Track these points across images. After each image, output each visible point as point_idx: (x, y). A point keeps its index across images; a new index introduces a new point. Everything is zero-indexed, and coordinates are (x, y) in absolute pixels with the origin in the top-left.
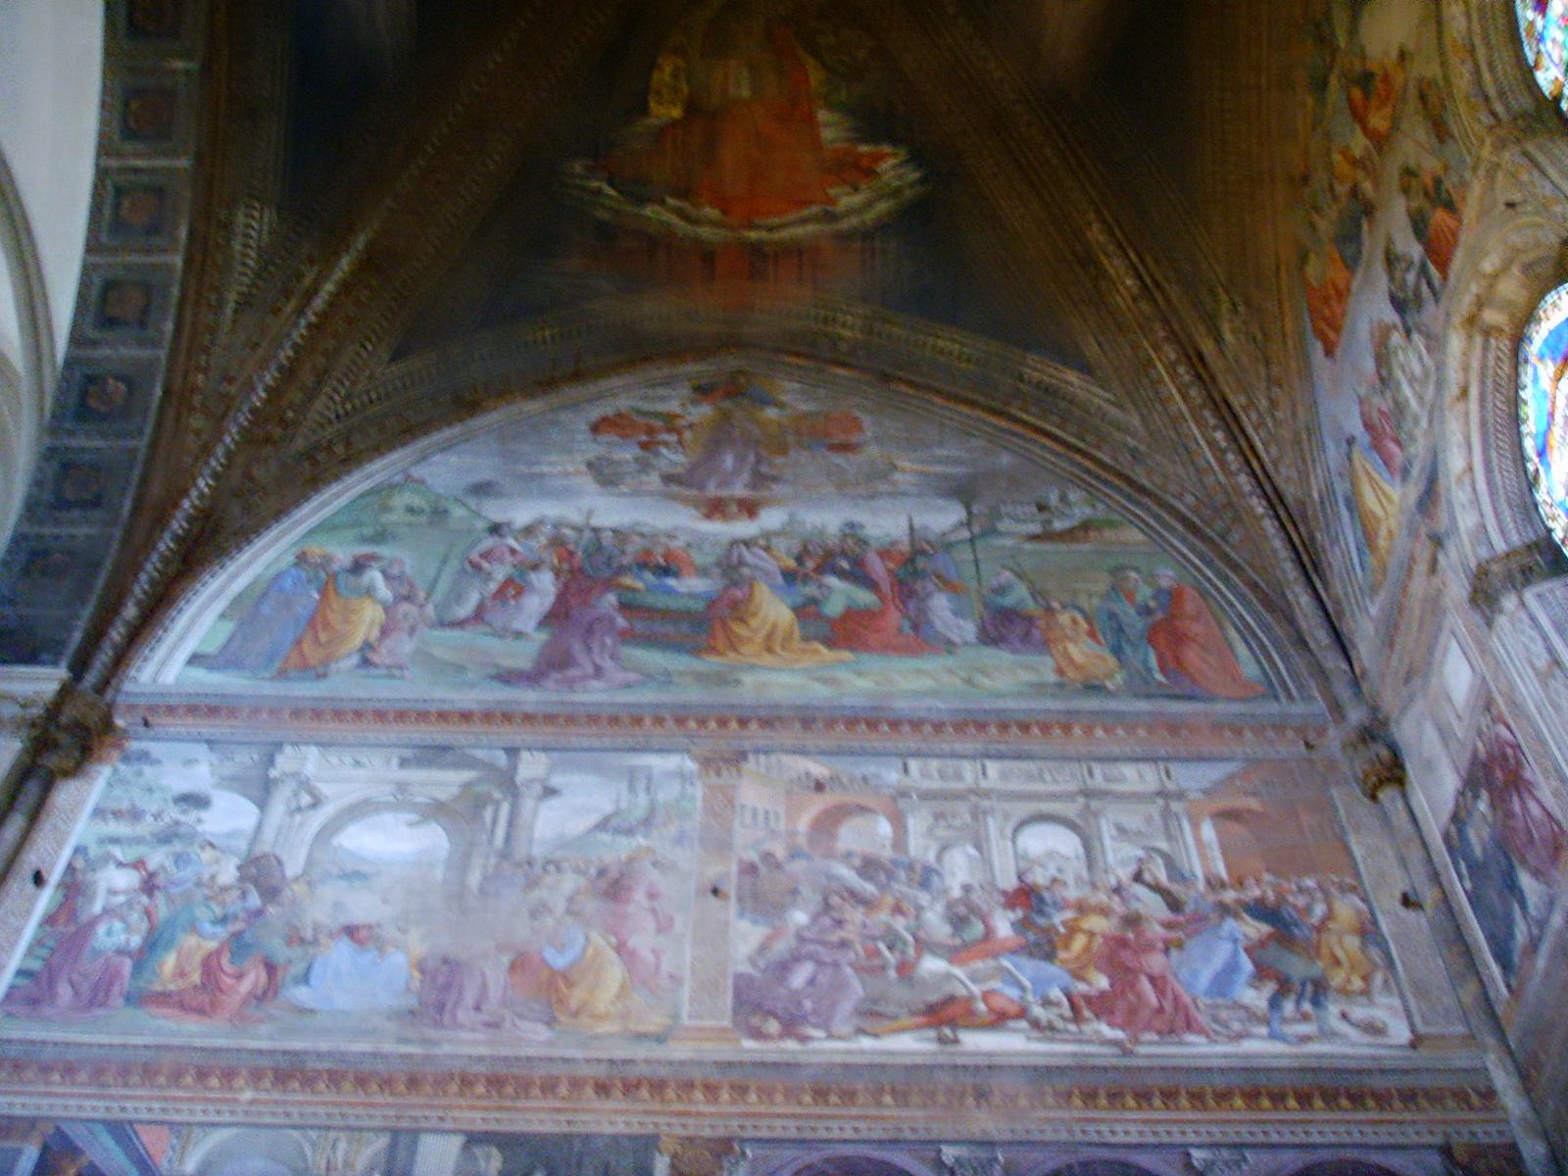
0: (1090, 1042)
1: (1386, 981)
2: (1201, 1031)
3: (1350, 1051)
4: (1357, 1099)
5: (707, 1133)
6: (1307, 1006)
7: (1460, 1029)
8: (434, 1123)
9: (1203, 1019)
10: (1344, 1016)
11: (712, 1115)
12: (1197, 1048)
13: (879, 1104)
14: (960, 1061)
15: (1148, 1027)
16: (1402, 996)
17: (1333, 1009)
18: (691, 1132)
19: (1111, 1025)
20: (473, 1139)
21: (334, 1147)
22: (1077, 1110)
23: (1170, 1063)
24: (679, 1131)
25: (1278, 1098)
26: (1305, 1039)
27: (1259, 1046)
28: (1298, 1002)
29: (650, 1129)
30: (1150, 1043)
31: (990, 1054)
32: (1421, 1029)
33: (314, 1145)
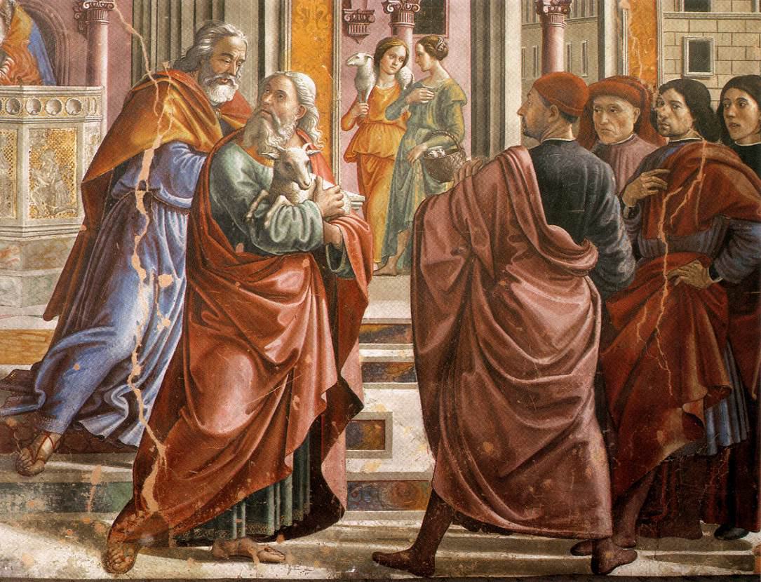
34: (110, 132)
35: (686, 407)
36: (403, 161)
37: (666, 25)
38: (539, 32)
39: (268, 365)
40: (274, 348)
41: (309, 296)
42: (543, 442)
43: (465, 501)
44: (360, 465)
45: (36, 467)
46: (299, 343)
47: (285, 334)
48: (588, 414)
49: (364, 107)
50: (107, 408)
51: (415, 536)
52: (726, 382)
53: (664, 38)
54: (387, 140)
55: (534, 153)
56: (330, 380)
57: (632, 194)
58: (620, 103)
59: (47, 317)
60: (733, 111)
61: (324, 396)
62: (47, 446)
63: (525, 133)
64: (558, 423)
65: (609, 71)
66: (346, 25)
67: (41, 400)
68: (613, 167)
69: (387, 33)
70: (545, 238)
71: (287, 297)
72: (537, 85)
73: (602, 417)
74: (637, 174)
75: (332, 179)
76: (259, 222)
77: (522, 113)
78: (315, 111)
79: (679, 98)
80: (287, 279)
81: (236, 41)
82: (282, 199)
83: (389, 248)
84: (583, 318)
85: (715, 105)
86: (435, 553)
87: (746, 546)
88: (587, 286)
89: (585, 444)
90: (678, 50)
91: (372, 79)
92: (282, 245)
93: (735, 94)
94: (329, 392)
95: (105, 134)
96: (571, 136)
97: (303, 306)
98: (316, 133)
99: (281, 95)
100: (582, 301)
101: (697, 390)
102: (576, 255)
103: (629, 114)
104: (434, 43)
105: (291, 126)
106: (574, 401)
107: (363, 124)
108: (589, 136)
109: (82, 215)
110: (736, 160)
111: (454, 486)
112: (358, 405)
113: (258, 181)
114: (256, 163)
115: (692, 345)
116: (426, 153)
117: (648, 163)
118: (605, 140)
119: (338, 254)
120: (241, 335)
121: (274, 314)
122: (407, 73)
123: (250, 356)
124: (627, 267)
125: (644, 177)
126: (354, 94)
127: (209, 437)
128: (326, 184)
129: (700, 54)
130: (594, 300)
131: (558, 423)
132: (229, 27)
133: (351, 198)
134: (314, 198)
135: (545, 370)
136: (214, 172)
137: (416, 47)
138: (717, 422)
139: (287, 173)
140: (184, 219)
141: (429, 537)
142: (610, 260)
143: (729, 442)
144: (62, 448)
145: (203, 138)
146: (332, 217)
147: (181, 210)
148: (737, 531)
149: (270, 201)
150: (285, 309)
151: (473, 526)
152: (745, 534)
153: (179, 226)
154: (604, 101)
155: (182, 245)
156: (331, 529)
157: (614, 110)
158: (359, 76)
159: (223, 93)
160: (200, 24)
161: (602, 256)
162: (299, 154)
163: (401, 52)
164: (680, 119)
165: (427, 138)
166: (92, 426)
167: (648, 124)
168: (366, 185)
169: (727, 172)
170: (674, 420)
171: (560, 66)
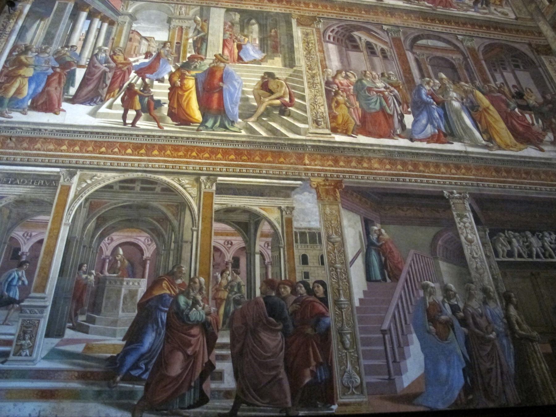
0: (422, 6)
1: (506, 3)
2: (455, 8)
3: (498, 18)
4: (503, 30)
5: (307, 15)
6: (484, 6)
7: (529, 17)
8: (214, 5)
9: (455, 5)
10: (495, 10)
11: (308, 10)
12: (454, 11)
13: (361, 13)
14: (384, 5)
15: (439, 5)
16: (511, 7)
17: (492, 8)
18: (302, 14)
19: (428, 3)
20: (228, 10)
21: (181, 9)
22: (421, 21)
23: (447, 14)
24: (297, 13)
25: (481, 27)
26: (486, 14)
27: (472, 13)
28: (482, 5)
29: (288, 12)
30: (440, 8)
31: (393, 5)
32: (518, 16)
33: (173, 7)
34: (147, 290)
35: (311, 368)
36: (228, 300)
37: (297, 268)
38: (265, 269)
39: (188, 356)
40: (190, 351)
41: (200, 336)
42: (270, 378)
43: (245, 395)
44: (214, 385)
45: (115, 385)
46: (197, 349)
47: (193, 347)
48: (282, 370)
49: (218, 286)
50: (138, 368)
51: (231, 408)
52: (321, 360)
53: (297, 271)
54: (224, 294)
55: (264, 299)
56: (206, 360)
57: (291, 309)
58: (286, 286)
59: (123, 340)
60: (316, 289)
61: (204, 365)
62: (118, 379)
63: (261, 293)
64: (274, 373)
65: (283, 278)
66: (213, 266)
67: (118, 365)
68: (286, 302)
69: (225, 268)
70: (268, 321)
71: (193, 336)
72: (264, 282)
73: (287, 369)
74: (292, 304)
75: (208, 304)
76: (187, 315)
77: (261, 288)
78: (204, 287)
79: (302, 285)
80: (195, 331)
81: (183, 269)
82: (194, 309)
83: (224, 323)
84: (280, 342)
85: (311, 287)
86: (237, 412)
87: (332, 410)
88: (280, 334)
89: (282, 379)
90: (301, 274)
91: (220, 279)
92: (193, 321)
93: (316, 284)
94: (206, 363)
95: (145, 290)
96: (274, 294)
97: (198, 339)
98: (204, 292)
99: (195, 283)
100: (279, 338)
101: (314, 363)
102: (276, 326)
103: (289, 289)
104: (237, 271)
105: (197, 290)
106: (278, 366)
107: (217, 290)
108: (279, 294)
109: (137, 312)
110: (319, 301)
111: (242, 391)
112: (214, 368)
113: (187, 304)
114: (187, 300)
115: (311, 349)
116: (234, 298)
117: (295, 302)
118: (283, 295)
119: (210, 324)
120: (180, 346)
121: (190, 341)
122: (230, 278)
123: (183, 353)
124: (291, 329)
125: (294, 305)
126: (215, 282)
127: (169, 377)
128: (206, 306)
129: (307, 275)
130: (282, 338)
131: (274, 373)
132: (182, 265)
133: (213, 309)
134: (203, 309)
135: (269, 357)
136: (176, 301)
137: (232, 271)
138: (320, 373)
139: (195, 303)
140: (166, 314)
141: (235, 408)
142: (285, 328)
143: (324, 377)
144: (123, 380)
145: (173, 293)
146: (208, 314)
147: (165, 311)
148: (329, 405)
149: (191, 309)
150: (193, 340)
151: (249, 404)
152: (331, 406)
153: (164, 316)
154: (282, 286)
155: (165, 322)
156: (205, 406)
157: (285, 288)
158: (216, 278)
159: (179, 281)
160: (174, 264)
161: (284, 326)
162: (199, 297)
163: (228, 272)
164: (302, 290)
165: (235, 294)
166: (134, 373)
167: (294, 291)
168: (218, 306)
169: (315, 303)
170: (308, 372)
171: (270, 277)
